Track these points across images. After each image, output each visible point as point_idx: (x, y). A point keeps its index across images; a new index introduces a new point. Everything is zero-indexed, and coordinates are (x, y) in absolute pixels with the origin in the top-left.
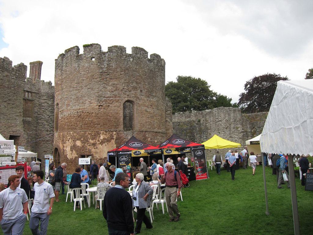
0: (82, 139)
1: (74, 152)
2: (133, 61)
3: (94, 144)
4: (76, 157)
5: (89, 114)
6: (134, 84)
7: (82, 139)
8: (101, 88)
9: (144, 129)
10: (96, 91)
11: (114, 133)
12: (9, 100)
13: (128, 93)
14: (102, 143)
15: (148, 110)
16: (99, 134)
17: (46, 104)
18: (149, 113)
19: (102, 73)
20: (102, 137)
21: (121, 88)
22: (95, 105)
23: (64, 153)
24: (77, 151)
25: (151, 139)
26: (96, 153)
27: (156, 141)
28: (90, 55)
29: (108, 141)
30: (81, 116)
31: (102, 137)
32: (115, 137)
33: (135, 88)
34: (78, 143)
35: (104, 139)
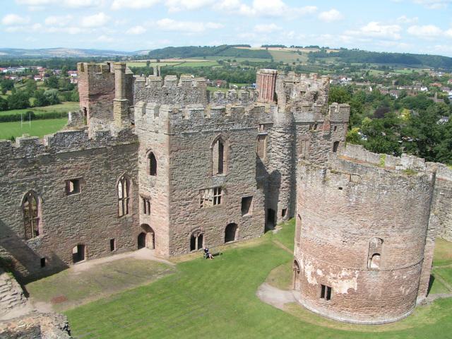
0: (323, 270)
1: (315, 279)
2: (386, 194)
3: (334, 278)
4: (316, 285)
5: (333, 248)
6: (386, 220)
7: (323, 270)
8: (347, 223)
9: (391, 267)
10: (341, 225)
11: (357, 271)
12: (242, 157)
13: (376, 231)
14: (343, 279)
15: (399, 246)
16: (340, 269)
17: (282, 139)
18: (400, 249)
19: (349, 208)
20: (344, 273)
21: (370, 225)
22: (339, 239)
23: (304, 274)
24: (317, 279)
25: (399, 276)
26: (336, 287)
27: (405, 277)
28: (338, 184)
29: (350, 278)
30: (324, 247)
31: (344, 273)
32: (357, 276)
33: (386, 225)
34: (319, 272)
35: (346, 276)
